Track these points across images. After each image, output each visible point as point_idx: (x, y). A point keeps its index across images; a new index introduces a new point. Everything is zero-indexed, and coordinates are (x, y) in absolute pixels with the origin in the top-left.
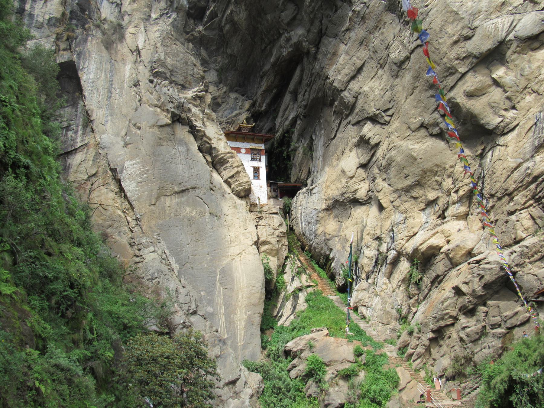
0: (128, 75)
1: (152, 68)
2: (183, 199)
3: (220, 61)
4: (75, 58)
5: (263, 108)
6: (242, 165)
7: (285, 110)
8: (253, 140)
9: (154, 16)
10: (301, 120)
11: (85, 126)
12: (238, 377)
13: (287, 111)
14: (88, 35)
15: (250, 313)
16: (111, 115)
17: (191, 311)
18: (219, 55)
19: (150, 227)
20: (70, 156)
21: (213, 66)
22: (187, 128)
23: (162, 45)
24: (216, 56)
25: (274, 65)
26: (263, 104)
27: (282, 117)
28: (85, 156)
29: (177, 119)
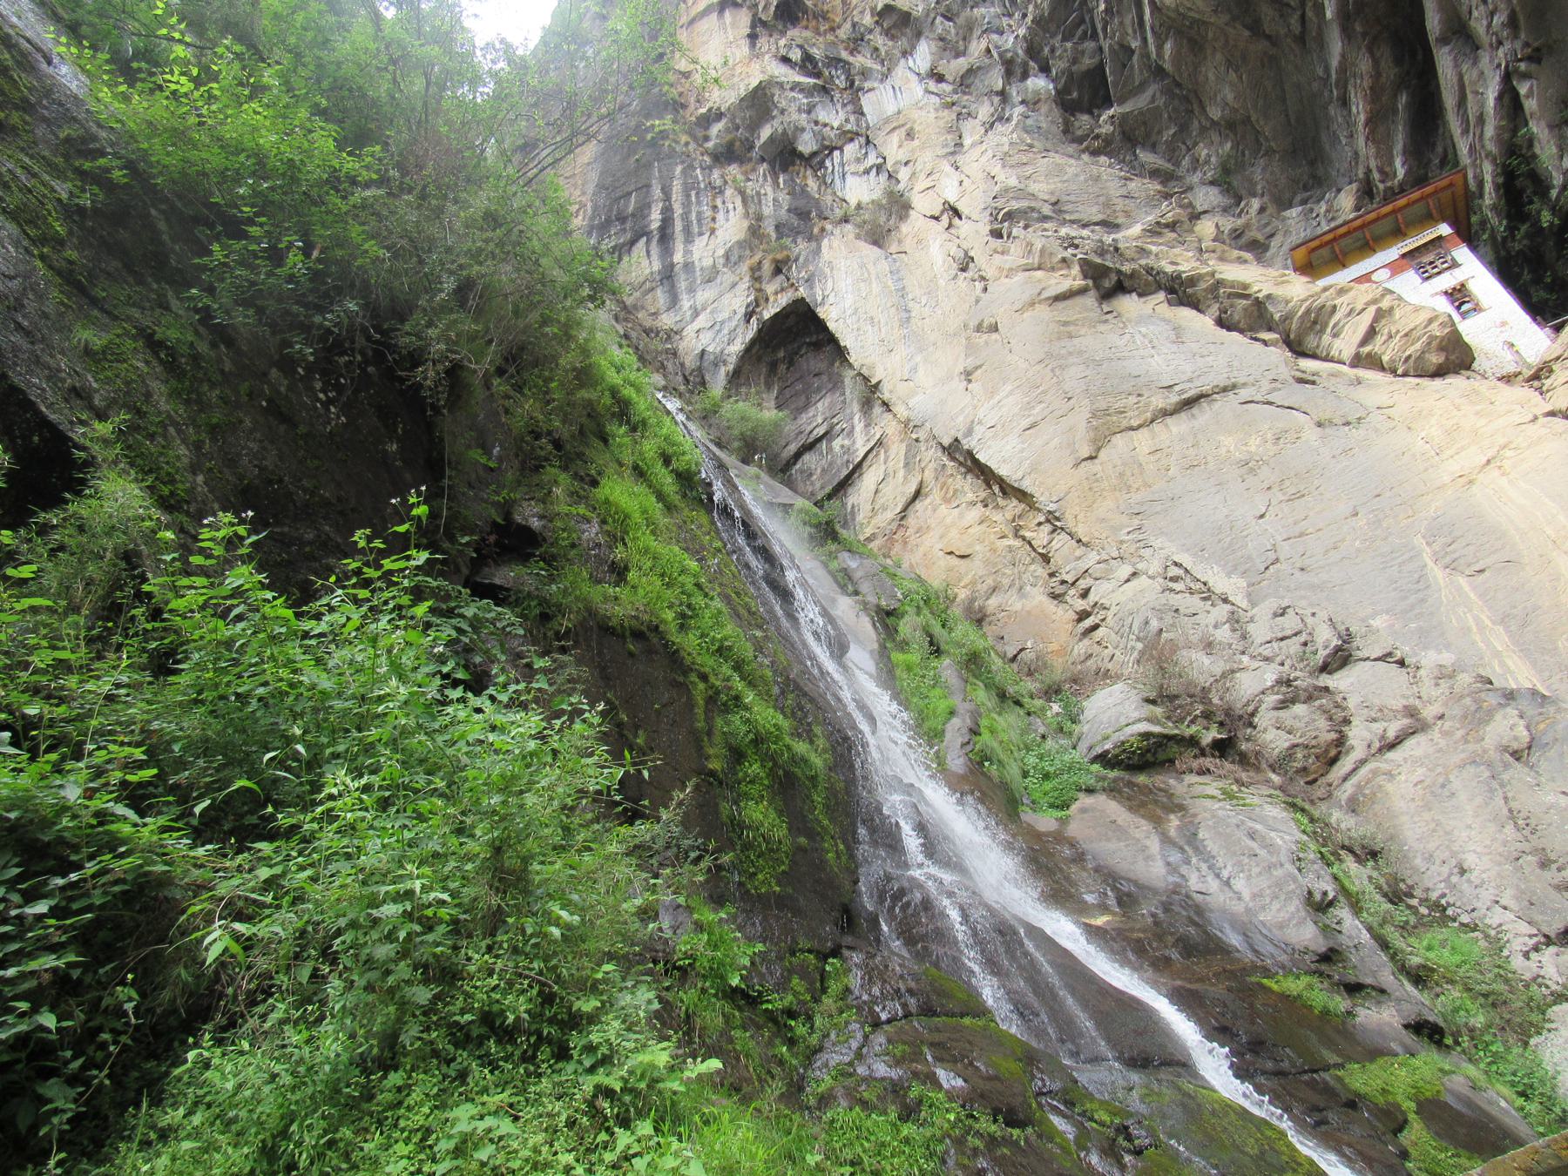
2: (1197, 423)
3: (1209, 156)
4: (802, 292)
5: (1401, 172)
8: (1398, 233)
10: (1525, 76)
11: (867, 404)
16: (921, 350)
18: (1196, 144)
20: (850, 490)
21: (1195, 178)
22: (1161, 296)
24: (1189, 150)
25: (1347, 32)
26: (1391, 163)
27: (1466, 131)
28: (883, 468)
29: (1110, 282)
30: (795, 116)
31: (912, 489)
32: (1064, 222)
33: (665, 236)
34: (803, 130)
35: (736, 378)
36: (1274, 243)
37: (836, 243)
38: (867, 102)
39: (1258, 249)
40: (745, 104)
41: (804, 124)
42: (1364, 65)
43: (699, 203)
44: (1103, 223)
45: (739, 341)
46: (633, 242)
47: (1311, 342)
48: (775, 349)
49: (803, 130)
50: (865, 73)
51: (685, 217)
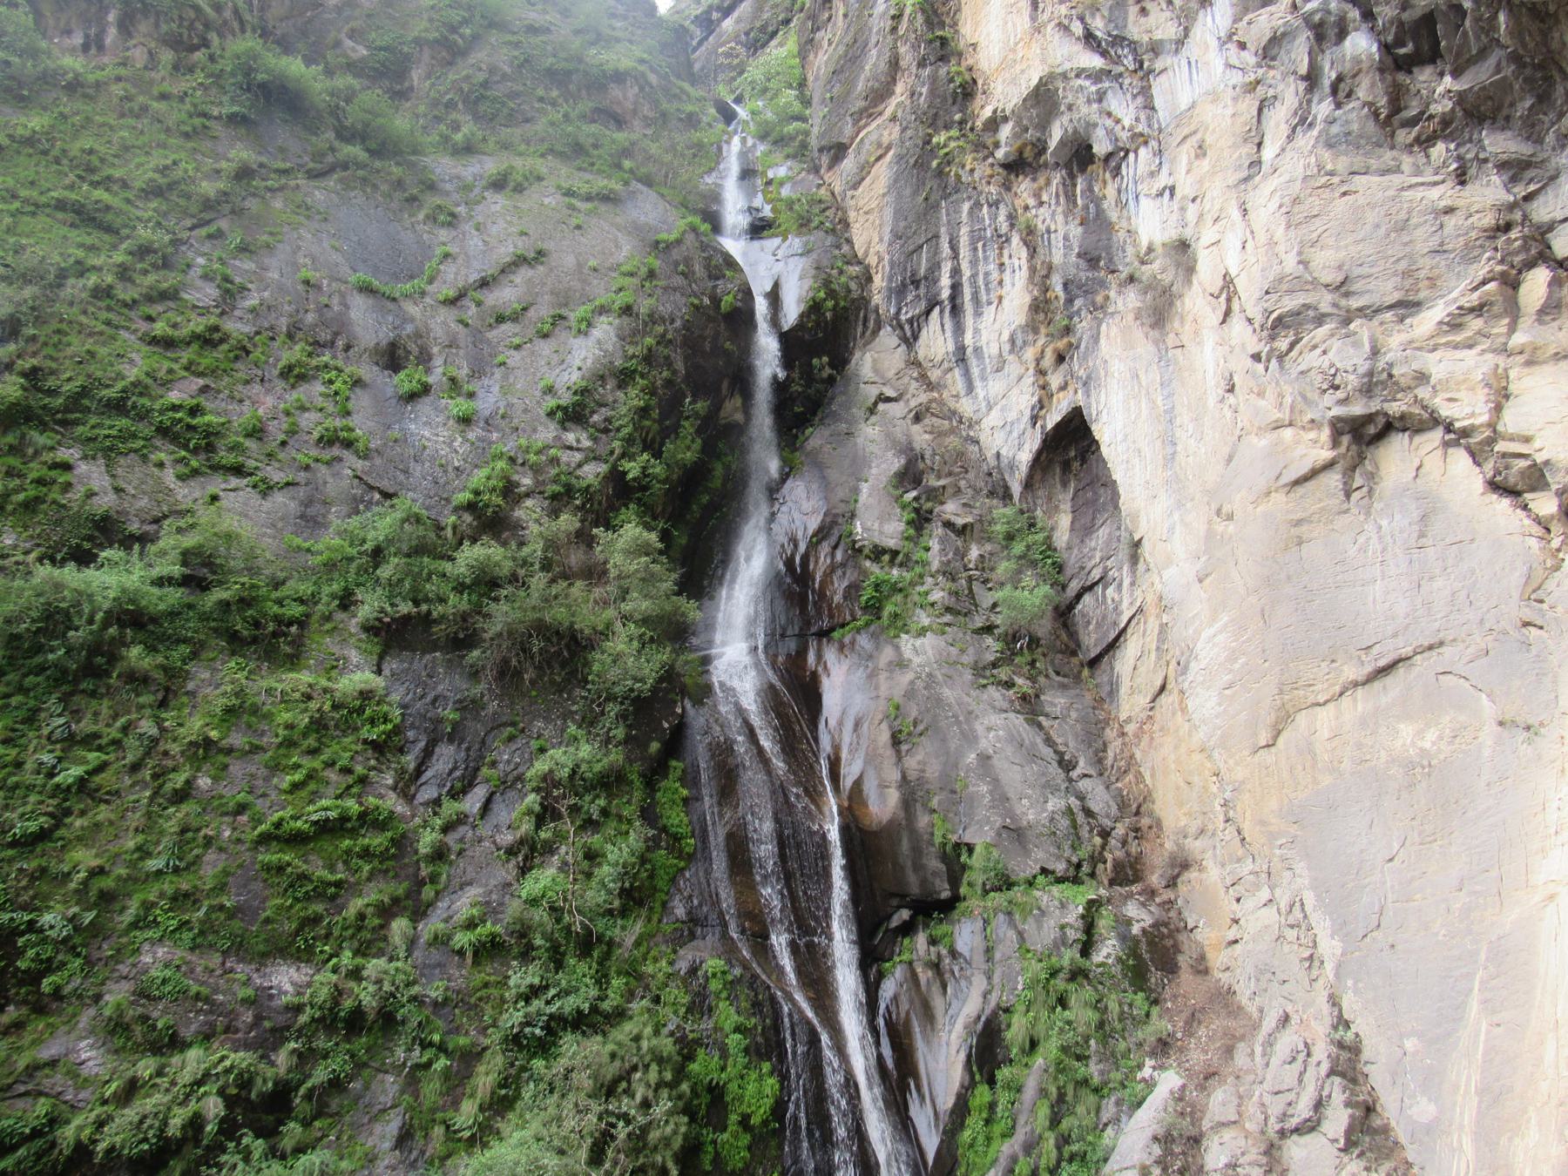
2: (1384, 700)
9: (1268, 153)
17: (1294, 1122)
19: (1263, 823)
20: (1118, 653)
23: (1288, 226)
30: (1084, 110)
31: (1159, 683)
33: (956, 310)
34: (1095, 125)
35: (1028, 485)
37: (1114, 330)
38: (1159, 87)
40: (1029, 103)
41: (1095, 118)
43: (986, 258)
45: (1027, 447)
46: (928, 312)
48: (1066, 449)
49: (1095, 125)
50: (1155, 49)
51: (974, 276)
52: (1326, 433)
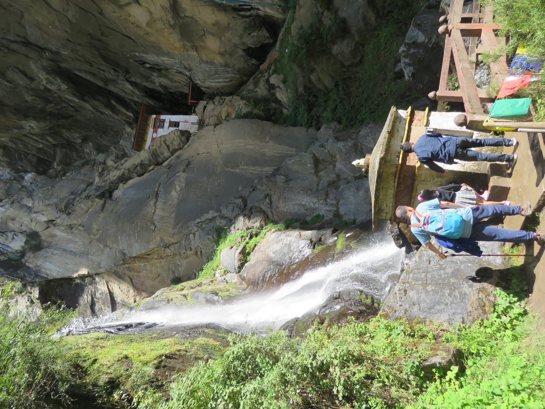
0: (64, 234)
1: (61, 211)
5: (131, 114)
6: (160, 137)
7: (125, 93)
10: (130, 78)
12: (312, 155)
13: (127, 91)
14: (25, 265)
15: (268, 137)
16: (87, 255)
18: (83, 151)
20: (116, 299)
21: (93, 157)
22: (121, 185)
23: (48, 200)
24: (84, 153)
25: (85, 101)
26: (127, 115)
27: (133, 97)
29: (107, 194)
32: (81, 194)
36: (126, 151)
37: (30, 261)
39: (125, 155)
42: (97, 103)
44: (88, 186)
47: (160, 160)
52: (97, 200)
